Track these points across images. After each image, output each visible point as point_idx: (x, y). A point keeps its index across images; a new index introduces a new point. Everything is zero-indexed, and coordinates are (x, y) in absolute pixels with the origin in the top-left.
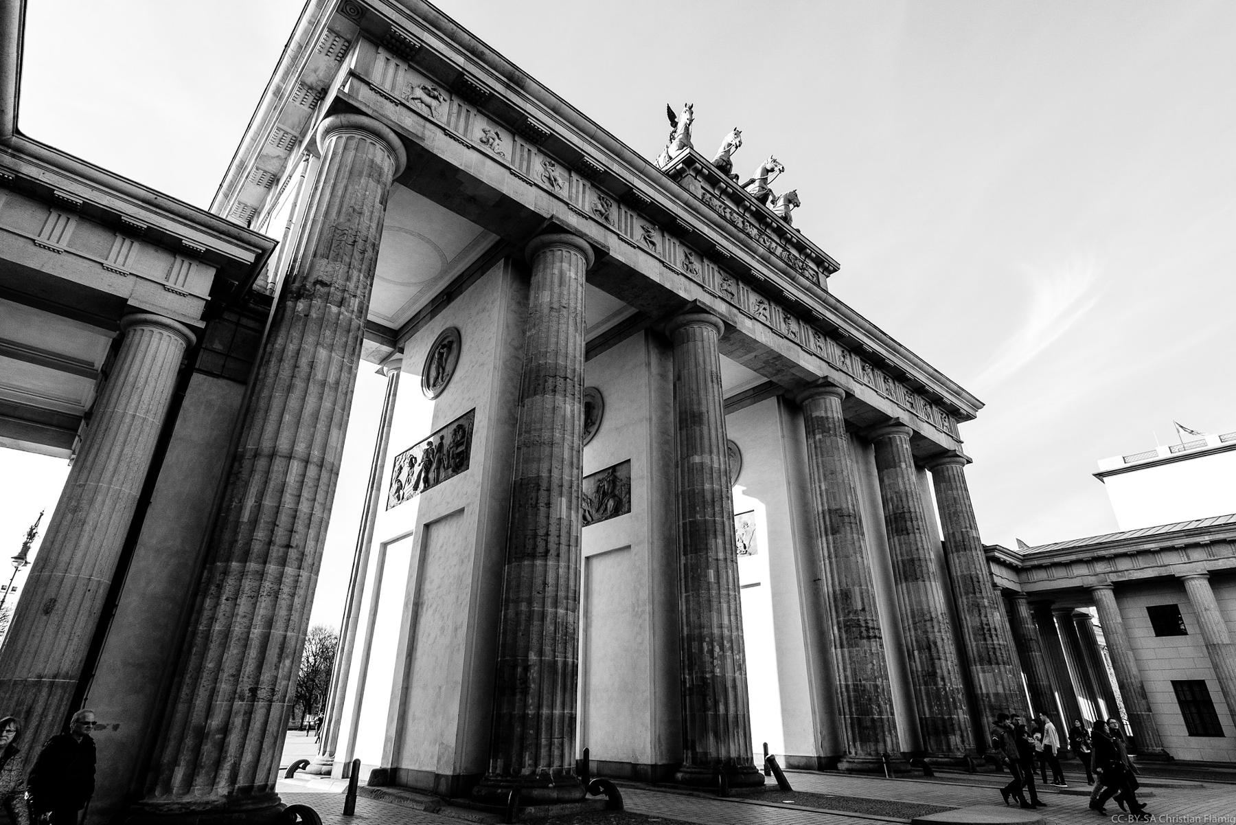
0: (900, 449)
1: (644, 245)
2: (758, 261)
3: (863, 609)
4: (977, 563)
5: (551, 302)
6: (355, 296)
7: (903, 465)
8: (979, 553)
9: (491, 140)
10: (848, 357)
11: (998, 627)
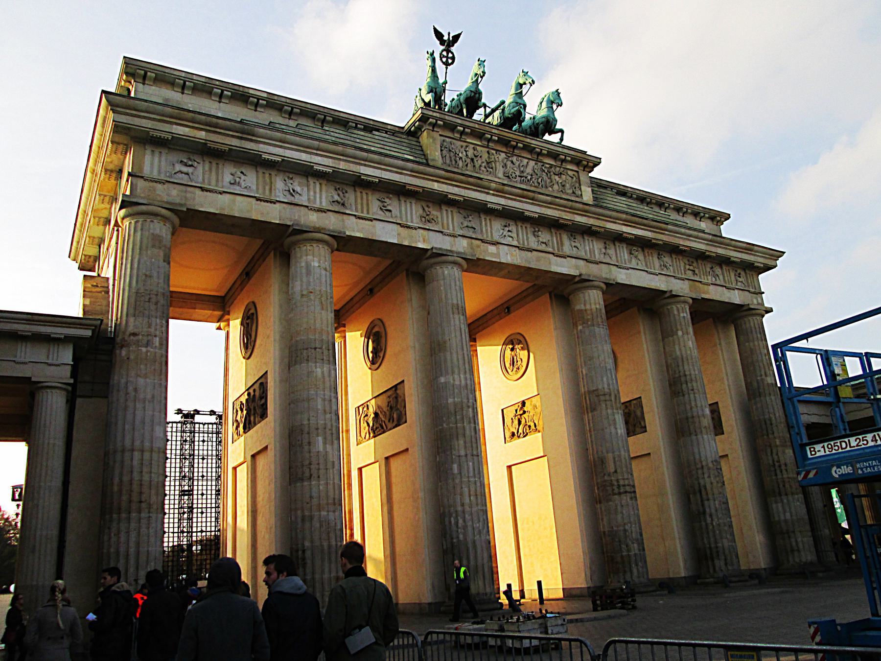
0: (677, 317)
1: (381, 215)
2: (493, 195)
3: (616, 472)
4: (770, 407)
5: (302, 291)
6: (155, 336)
7: (680, 333)
8: (773, 398)
9: (238, 180)
10: (612, 246)
11: (788, 462)
